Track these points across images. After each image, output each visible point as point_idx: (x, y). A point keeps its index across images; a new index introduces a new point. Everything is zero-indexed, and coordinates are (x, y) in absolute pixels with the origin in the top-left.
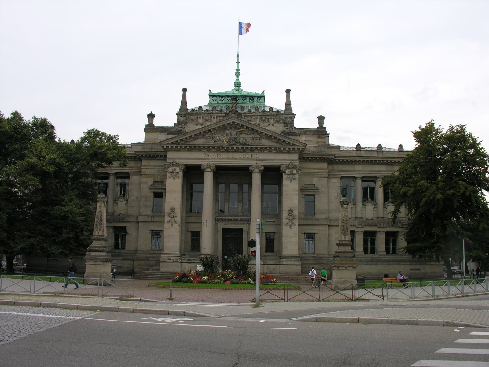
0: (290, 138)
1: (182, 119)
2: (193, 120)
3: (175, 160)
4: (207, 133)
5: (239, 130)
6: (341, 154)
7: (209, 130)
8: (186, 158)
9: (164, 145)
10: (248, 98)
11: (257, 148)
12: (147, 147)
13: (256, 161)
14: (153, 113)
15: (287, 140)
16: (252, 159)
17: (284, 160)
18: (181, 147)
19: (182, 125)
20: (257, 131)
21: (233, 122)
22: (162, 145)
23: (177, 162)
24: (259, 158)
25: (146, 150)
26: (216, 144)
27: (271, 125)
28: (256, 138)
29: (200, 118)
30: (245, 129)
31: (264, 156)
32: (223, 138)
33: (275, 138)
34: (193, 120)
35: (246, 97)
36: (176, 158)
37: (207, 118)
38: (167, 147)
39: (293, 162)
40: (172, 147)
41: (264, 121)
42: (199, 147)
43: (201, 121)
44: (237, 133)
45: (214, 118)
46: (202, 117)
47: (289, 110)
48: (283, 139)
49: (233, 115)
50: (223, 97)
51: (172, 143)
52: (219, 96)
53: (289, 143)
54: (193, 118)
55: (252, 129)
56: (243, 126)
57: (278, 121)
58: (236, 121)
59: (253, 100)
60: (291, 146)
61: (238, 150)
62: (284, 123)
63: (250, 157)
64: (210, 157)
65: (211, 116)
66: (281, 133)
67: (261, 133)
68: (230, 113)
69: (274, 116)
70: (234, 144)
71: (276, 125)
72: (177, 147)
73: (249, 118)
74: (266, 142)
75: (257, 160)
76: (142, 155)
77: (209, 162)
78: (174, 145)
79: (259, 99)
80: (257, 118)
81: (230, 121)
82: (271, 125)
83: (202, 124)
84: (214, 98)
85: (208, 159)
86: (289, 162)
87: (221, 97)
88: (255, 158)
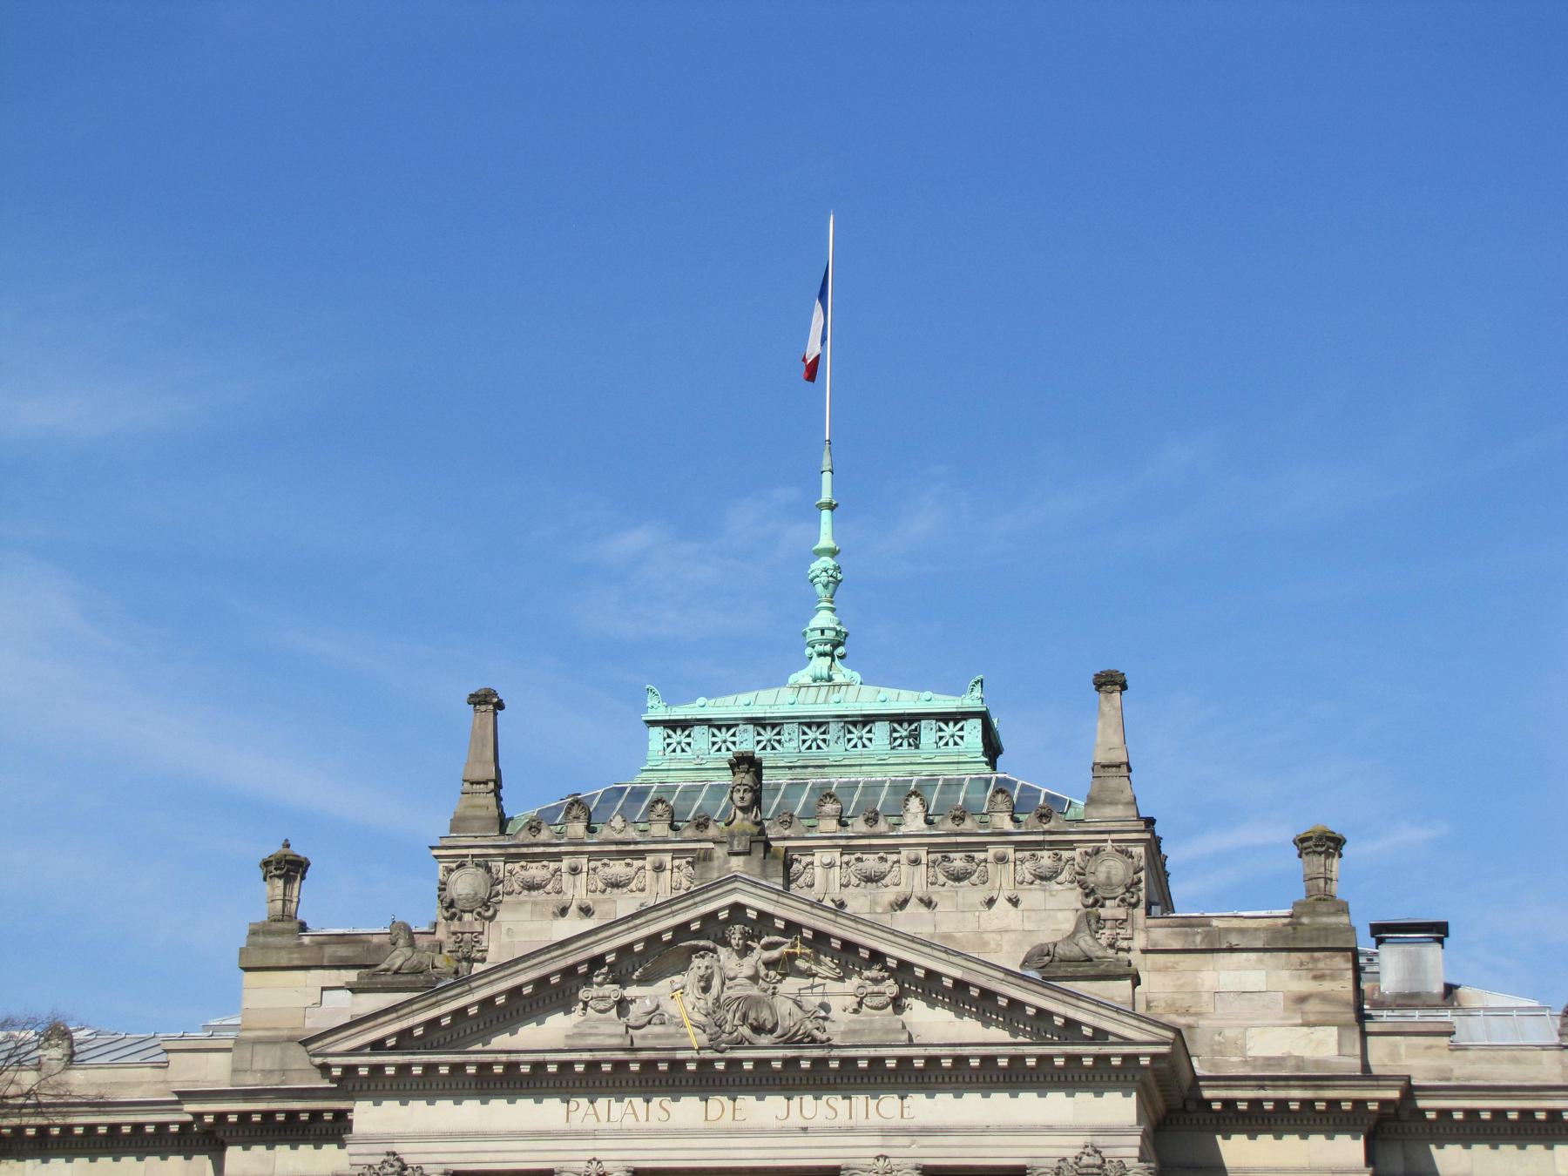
0: (1078, 996)
1: (465, 884)
2: (531, 887)
3: (397, 1148)
4: (587, 980)
5: (775, 954)
6: (1464, 1069)
7: (596, 962)
8: (464, 1136)
9: (331, 1060)
10: (881, 730)
11: (877, 1062)
12: (258, 1065)
13: (877, 1141)
14: (260, 873)
15: (1061, 1009)
16: (850, 1130)
17: (1050, 1129)
18: (430, 1068)
19: (467, 917)
20: (877, 957)
21: (737, 909)
22: (318, 1060)
23: (407, 1159)
24: (896, 1122)
25: (251, 1081)
26: (637, 1043)
27: (1002, 904)
28: (877, 1001)
29: (575, 871)
30: (805, 942)
31: (924, 1108)
32: (676, 1008)
33: (988, 995)
34: (531, 887)
35: (867, 720)
36: (405, 1138)
37: (618, 868)
38: (350, 1070)
39: (1100, 1141)
40: (377, 1069)
41: (958, 877)
42: (539, 1066)
43: (577, 890)
44: (763, 971)
45: (659, 868)
46: (583, 861)
47: (1113, 803)
48: (1035, 999)
49: (737, 863)
50: (729, 727)
51: (378, 1046)
52: (708, 722)
53: (1072, 1025)
54: (536, 871)
55: (849, 947)
56: (792, 928)
57: (1043, 878)
58: (756, 902)
59: (915, 737)
60: (1090, 1041)
61: (764, 1080)
62: (1082, 885)
63: (843, 1119)
64: (604, 1125)
65: (641, 855)
66: (1025, 963)
67: (905, 966)
68: (720, 852)
69: (1019, 846)
70: (739, 1043)
71: (1033, 897)
72: (404, 1069)
73: (871, 862)
74: (935, 1026)
75: (886, 1132)
76: (221, 1117)
77: (599, 1155)
78: (391, 1060)
79: (950, 729)
80: (916, 862)
81: (719, 903)
82: (1002, 904)
83: (586, 911)
84: (678, 737)
85: (594, 1134)
86: (1080, 1141)
87: (719, 728)
88: (875, 1120)
